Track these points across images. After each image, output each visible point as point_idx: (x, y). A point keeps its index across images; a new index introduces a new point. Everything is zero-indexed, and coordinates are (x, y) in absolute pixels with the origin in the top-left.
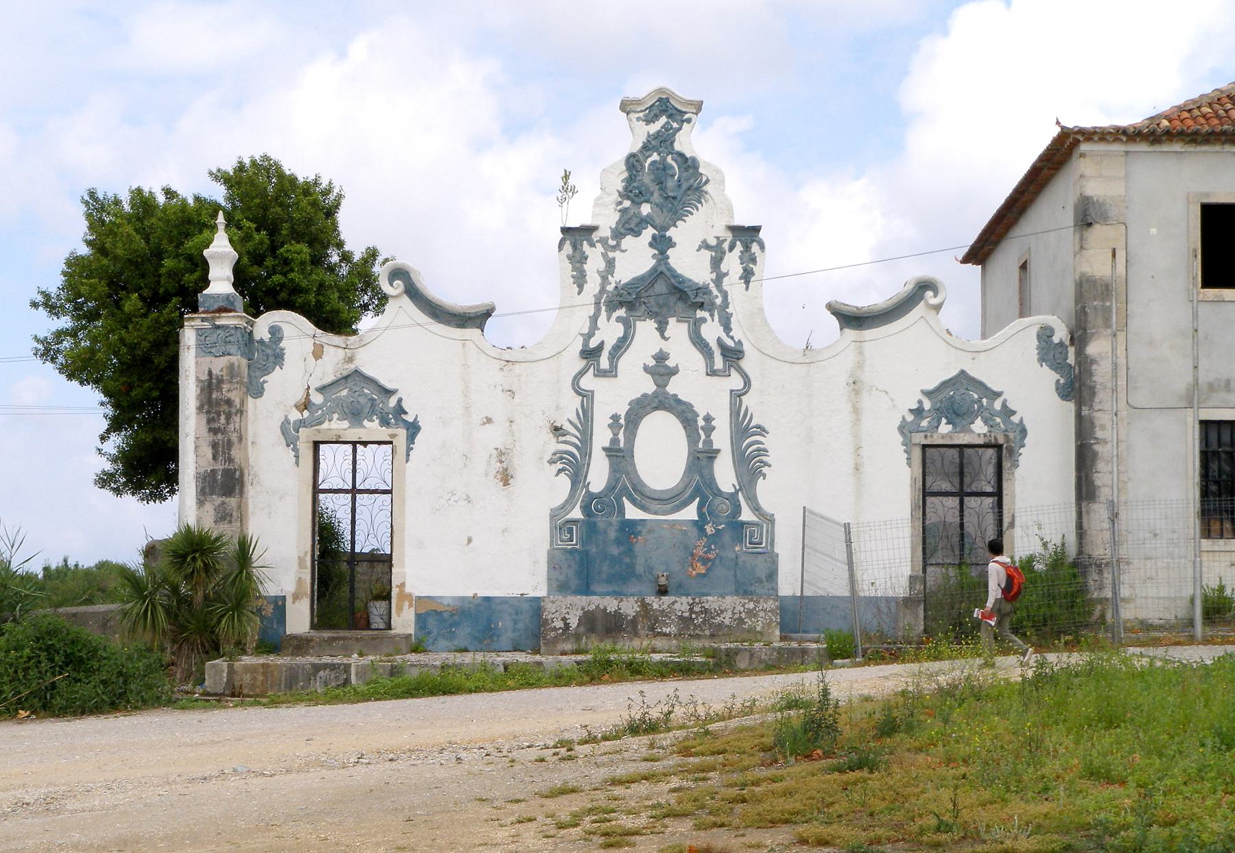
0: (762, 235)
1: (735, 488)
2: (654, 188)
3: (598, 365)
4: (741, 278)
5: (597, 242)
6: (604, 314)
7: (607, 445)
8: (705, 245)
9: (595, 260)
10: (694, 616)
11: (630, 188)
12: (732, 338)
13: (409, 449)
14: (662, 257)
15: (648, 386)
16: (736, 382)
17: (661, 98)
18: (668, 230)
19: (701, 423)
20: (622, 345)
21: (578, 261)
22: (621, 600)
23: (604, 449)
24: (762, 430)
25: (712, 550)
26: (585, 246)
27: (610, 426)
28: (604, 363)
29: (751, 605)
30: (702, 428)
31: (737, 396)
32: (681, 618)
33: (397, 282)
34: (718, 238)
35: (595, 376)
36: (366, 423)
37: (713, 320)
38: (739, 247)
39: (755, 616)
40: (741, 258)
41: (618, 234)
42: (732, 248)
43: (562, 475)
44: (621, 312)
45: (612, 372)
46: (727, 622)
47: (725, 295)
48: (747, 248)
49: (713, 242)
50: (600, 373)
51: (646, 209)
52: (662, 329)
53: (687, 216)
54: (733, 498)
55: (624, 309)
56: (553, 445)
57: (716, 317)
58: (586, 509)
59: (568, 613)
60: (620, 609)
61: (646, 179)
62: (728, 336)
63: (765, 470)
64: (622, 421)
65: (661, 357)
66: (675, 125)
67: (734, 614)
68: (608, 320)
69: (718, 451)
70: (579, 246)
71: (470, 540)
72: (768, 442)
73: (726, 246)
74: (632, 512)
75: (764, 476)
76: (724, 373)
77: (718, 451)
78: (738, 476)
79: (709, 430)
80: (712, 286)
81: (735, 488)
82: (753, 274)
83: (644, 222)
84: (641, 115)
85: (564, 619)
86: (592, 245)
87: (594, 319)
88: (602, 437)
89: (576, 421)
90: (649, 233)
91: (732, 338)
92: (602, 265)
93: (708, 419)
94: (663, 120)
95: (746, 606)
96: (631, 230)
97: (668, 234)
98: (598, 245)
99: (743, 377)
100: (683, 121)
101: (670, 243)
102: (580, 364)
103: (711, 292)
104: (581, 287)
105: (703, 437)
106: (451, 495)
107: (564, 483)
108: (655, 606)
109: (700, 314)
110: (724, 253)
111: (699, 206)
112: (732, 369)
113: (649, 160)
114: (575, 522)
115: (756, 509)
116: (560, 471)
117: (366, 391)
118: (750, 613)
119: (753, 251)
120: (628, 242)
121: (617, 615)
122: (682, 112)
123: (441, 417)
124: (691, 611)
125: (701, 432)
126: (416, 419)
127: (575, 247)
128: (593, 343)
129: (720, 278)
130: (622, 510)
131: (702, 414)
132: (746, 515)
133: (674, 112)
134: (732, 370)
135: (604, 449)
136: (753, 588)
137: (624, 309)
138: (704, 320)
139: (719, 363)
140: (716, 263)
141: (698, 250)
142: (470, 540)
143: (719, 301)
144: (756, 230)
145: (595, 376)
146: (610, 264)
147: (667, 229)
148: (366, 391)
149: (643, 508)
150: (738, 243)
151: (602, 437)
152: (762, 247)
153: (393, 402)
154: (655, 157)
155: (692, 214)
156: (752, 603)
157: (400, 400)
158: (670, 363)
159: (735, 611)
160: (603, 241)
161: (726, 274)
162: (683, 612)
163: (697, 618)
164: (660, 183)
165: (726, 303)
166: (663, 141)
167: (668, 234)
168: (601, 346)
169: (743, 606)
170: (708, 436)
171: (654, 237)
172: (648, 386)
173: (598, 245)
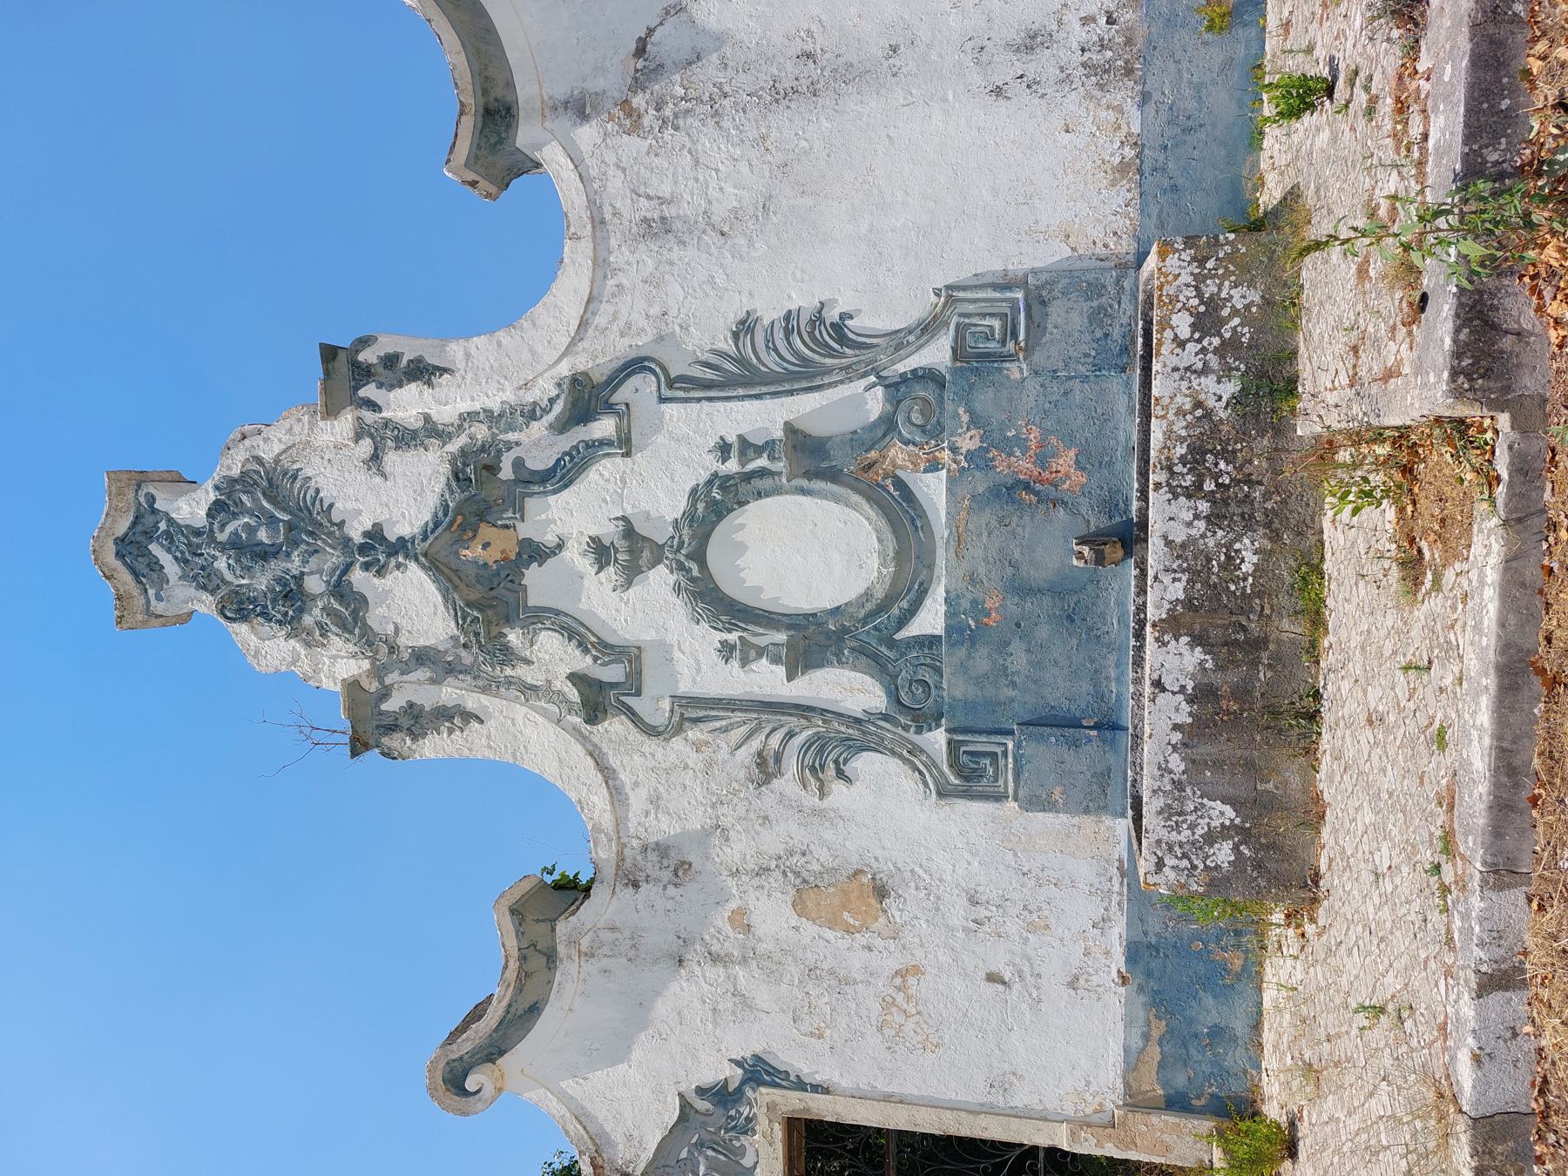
0: (345, 342)
1: (874, 385)
2: (276, 567)
3: (613, 685)
4: (429, 383)
5: (381, 682)
6: (521, 671)
7: (781, 670)
8: (376, 458)
9: (411, 690)
10: (1209, 486)
11: (279, 616)
12: (552, 401)
13: (800, 1085)
14: (401, 547)
15: (660, 579)
16: (639, 391)
17: (117, 554)
18: (350, 539)
19: (732, 466)
20: (575, 632)
21: (417, 721)
22: (1158, 684)
23: (790, 678)
24: (745, 327)
25: (1017, 436)
26: (392, 705)
27: (745, 662)
28: (613, 673)
29: (1182, 324)
30: (743, 464)
31: (679, 387)
32: (1213, 520)
33: (471, 1084)
34: (358, 437)
35: (638, 694)
36: (747, 1162)
37: (518, 444)
38: (369, 391)
39: (1213, 304)
40: (391, 387)
41: (370, 641)
42: (373, 406)
43: (847, 769)
44: (514, 637)
45: (630, 656)
46: (1230, 388)
47: (470, 417)
48: (363, 373)
49: (366, 446)
50: (634, 685)
51: (314, 585)
52: (535, 553)
53: (321, 500)
54: (897, 388)
55: (506, 630)
56: (787, 782)
57: (512, 436)
58: (924, 719)
59: (1192, 827)
60: (1183, 688)
61: (261, 581)
62: (546, 411)
63: (832, 315)
64: (733, 637)
65: (601, 552)
66: (163, 526)
67: (1205, 371)
68: (528, 662)
69: (790, 428)
70: (388, 721)
71: (993, 978)
72: (770, 313)
73: (369, 416)
74: (930, 620)
75: (844, 316)
76: (623, 413)
77: (790, 428)
78: (850, 373)
79: (747, 447)
80: (454, 447)
81: (874, 385)
82: (419, 360)
83: (340, 589)
84: (151, 592)
85: (1211, 838)
86: (385, 694)
87: (529, 690)
88: (768, 679)
89: (737, 734)
90: (358, 577)
91: (552, 401)
92: (423, 674)
93: (724, 449)
94: (154, 548)
95: (1185, 332)
96: (355, 613)
97: (358, 538)
98: (388, 681)
99: (628, 376)
100: (154, 511)
101: (375, 534)
102: (616, 726)
103: (463, 452)
104: (468, 716)
105: (762, 462)
106: (894, 1009)
107: (866, 764)
108: (1177, 591)
109: (506, 472)
110: (387, 423)
111: (301, 475)
112: (614, 399)
113: (229, 576)
114: (952, 746)
115: (927, 329)
116: (840, 774)
117: (684, 1154)
118: (1207, 321)
119: (375, 361)
120: (377, 617)
121: (1202, 694)
122: (138, 510)
123: (734, 1013)
124: (1194, 492)
125: (751, 466)
126: (738, 1063)
127: (392, 728)
128: (573, 694)
129: (432, 431)
130: (933, 641)
131: (713, 464)
132: (937, 354)
133: (139, 528)
134: (617, 397)
135: (790, 678)
136: (1116, 333)
137: (506, 630)
138: (518, 464)
139: (605, 427)
140: (407, 438)
141: (384, 476)
142: (993, 978)
143: (481, 432)
144: (329, 353)
145: (638, 694)
146: (422, 657)
147: (347, 541)
148: (684, 1154)
149: (922, 593)
150: (362, 393)
151: (768, 679)
152: (365, 342)
153: (702, 1105)
154: (221, 564)
155: (318, 491)
156: (1175, 320)
157: (701, 1091)
158: (609, 531)
159: (1200, 365)
160: (378, 672)
161: (427, 418)
162: (1196, 517)
163: (1216, 476)
164: (264, 554)
165: (490, 416)
166: (188, 542)
167: (358, 538)
168: (575, 678)
169: (1182, 344)
170: (759, 450)
171: (366, 567)
172: (660, 579)
173: (388, 681)
